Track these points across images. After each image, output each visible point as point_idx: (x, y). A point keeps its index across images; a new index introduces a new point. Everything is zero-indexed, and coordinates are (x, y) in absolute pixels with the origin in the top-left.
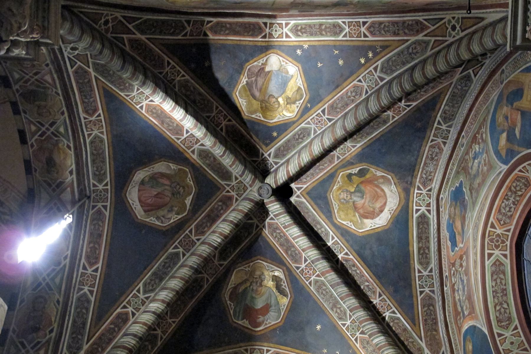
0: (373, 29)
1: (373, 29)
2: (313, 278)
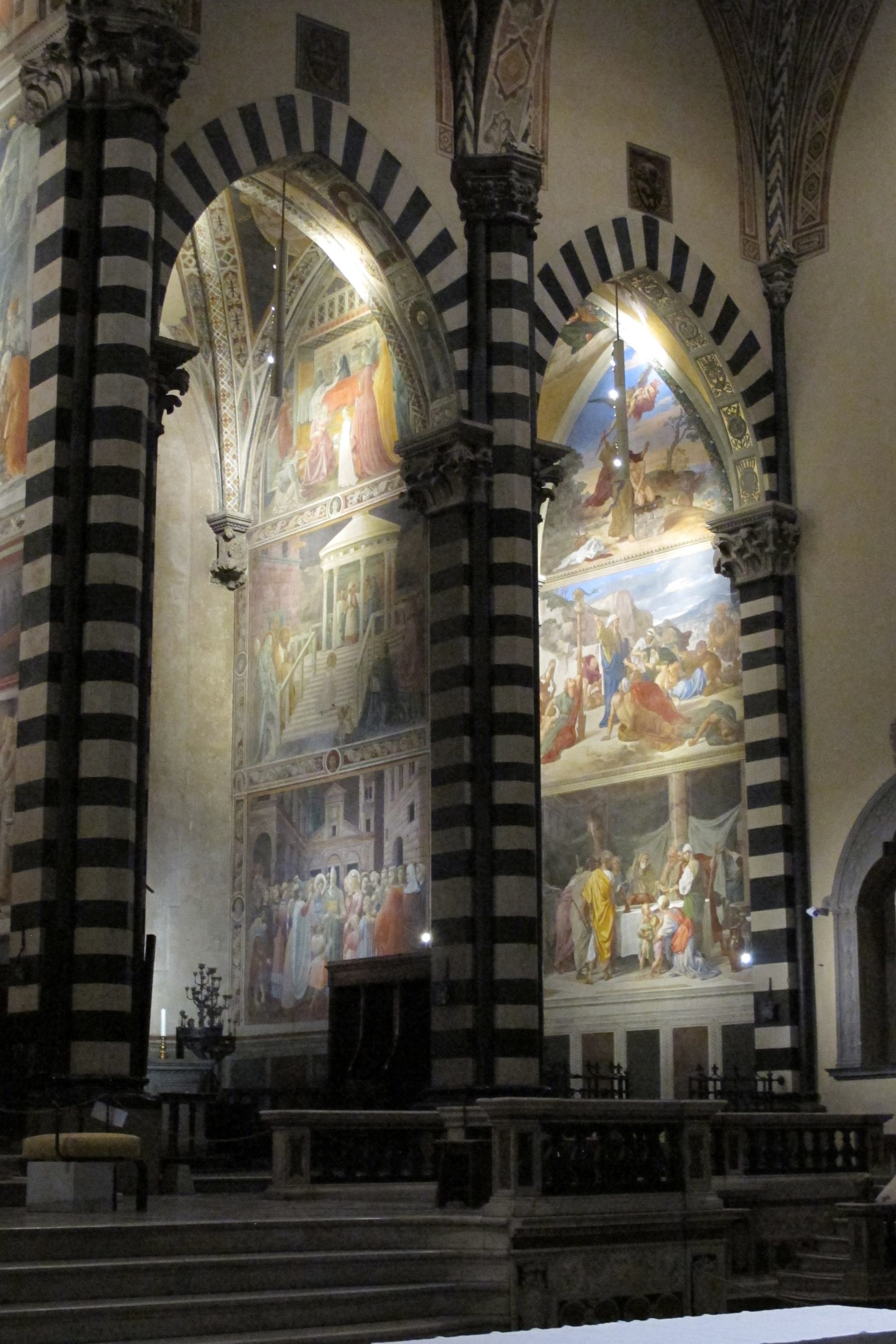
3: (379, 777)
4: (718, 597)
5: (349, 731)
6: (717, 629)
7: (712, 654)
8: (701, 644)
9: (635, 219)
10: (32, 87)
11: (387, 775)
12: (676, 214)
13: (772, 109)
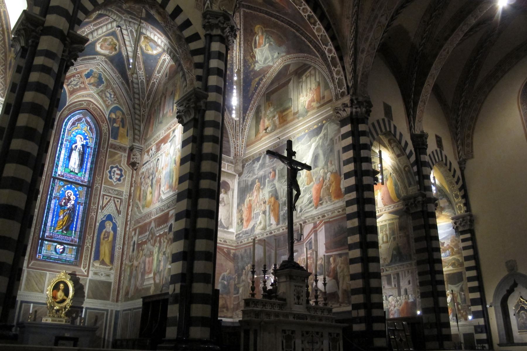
0: (154, 83)
1: (154, 83)
2: (87, 30)
3: (398, 274)
4: (452, 234)
5: (387, 263)
6: (452, 241)
7: (451, 247)
8: (448, 245)
9: (438, 150)
10: (338, 113)
11: (400, 273)
12: (444, 149)
13: (457, 129)
